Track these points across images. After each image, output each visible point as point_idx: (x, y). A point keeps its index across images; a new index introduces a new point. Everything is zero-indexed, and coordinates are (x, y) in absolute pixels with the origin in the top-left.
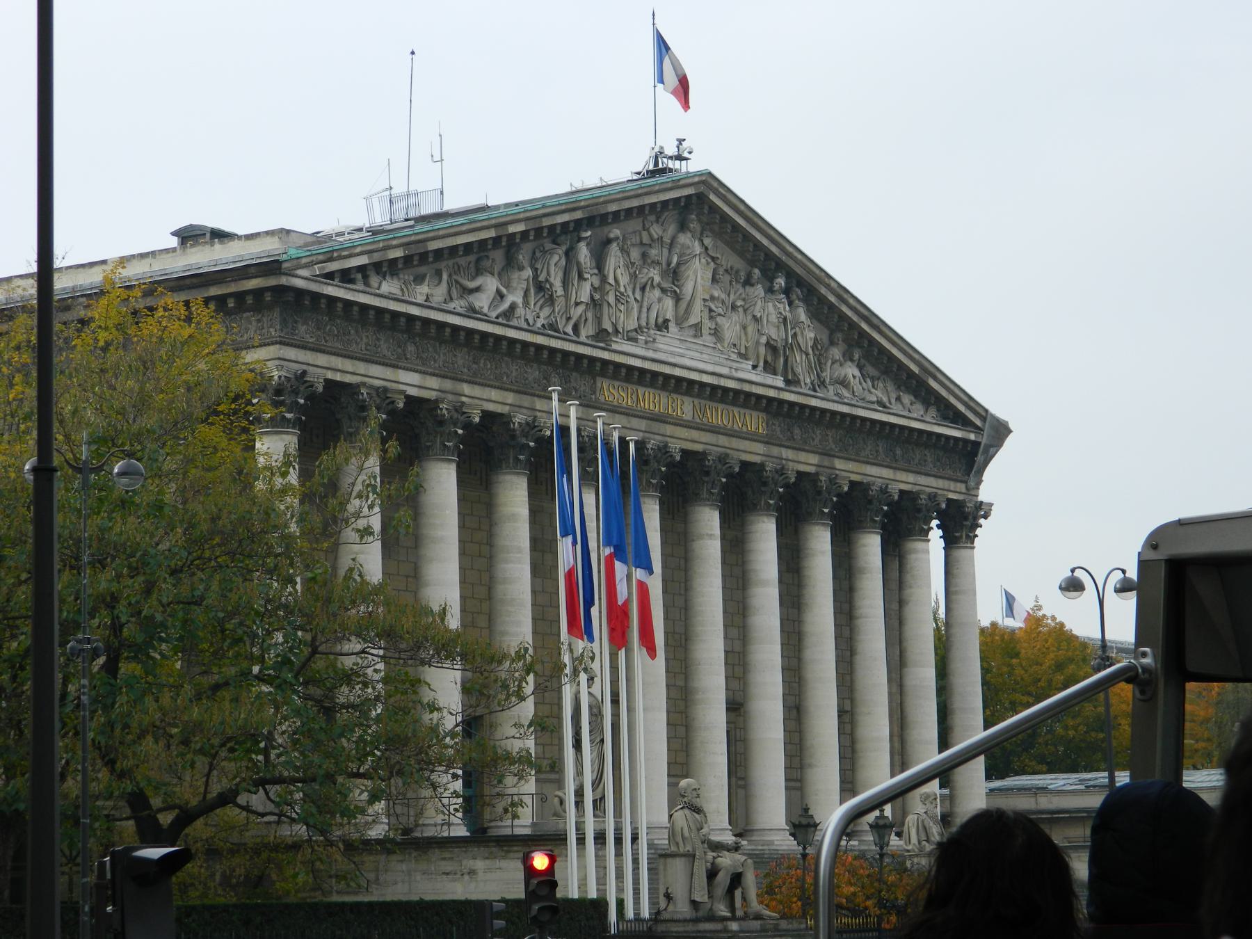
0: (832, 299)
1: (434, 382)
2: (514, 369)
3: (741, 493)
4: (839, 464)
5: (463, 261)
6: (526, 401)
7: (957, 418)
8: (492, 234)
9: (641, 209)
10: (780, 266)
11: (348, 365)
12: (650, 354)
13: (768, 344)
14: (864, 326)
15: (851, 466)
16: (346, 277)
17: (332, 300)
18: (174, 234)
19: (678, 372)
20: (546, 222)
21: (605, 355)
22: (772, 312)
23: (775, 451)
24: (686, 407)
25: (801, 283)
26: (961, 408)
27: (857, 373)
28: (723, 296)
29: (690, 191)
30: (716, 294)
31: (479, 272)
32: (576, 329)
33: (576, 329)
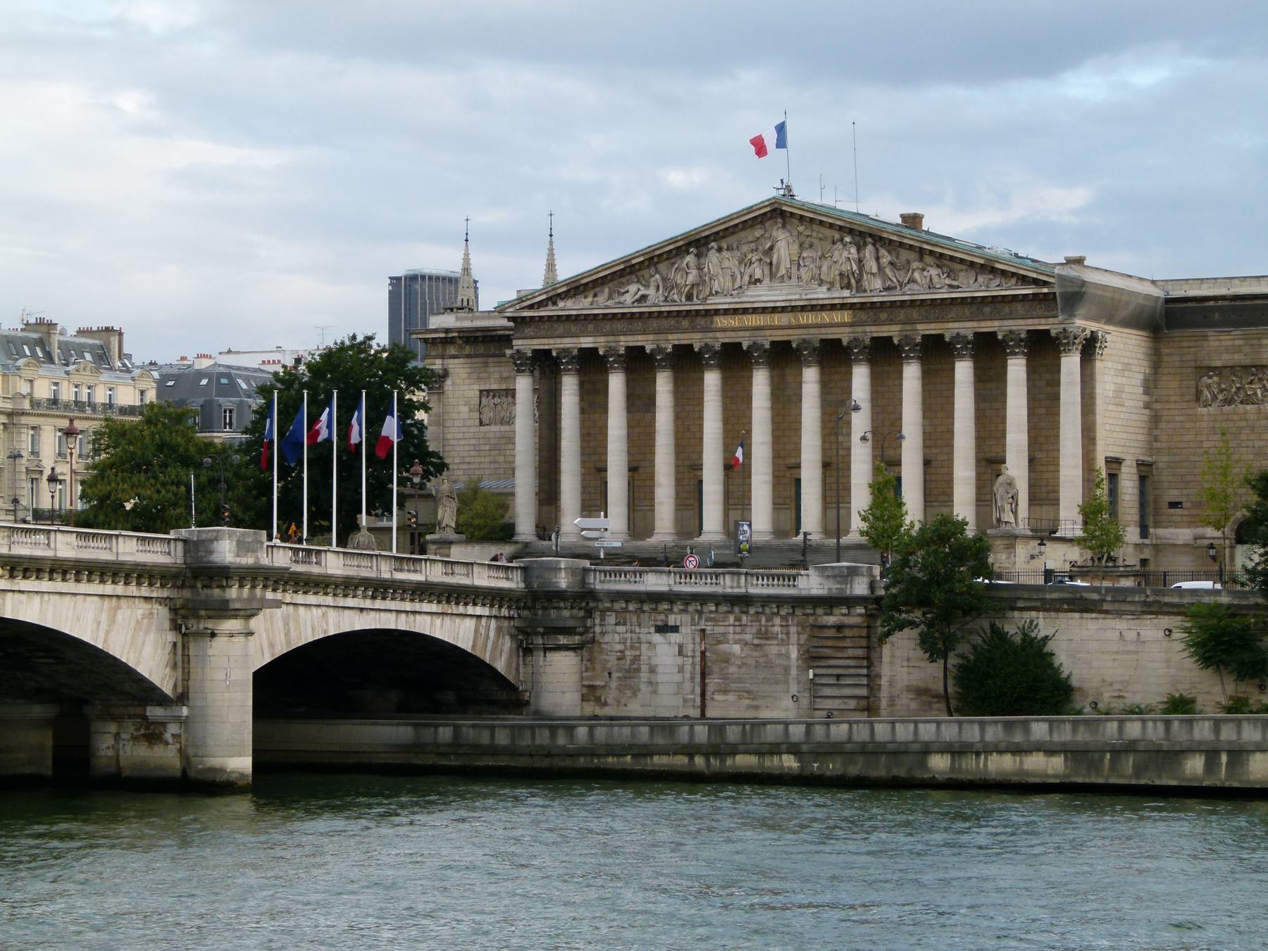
0: (895, 238)
1: (602, 339)
2: (654, 324)
3: (834, 356)
4: (919, 327)
5: (623, 280)
6: (662, 337)
7: (1036, 282)
8: (622, 266)
9: (736, 225)
10: (851, 232)
11: (551, 341)
12: (736, 300)
13: (841, 274)
14: (925, 246)
15: (932, 326)
16: (541, 304)
17: (532, 317)
18: (902, 216)
19: (756, 305)
20: (657, 253)
21: (701, 307)
22: (845, 256)
23: (860, 329)
24: (784, 319)
25: (871, 235)
26: (1035, 276)
27: (939, 271)
28: (814, 255)
29: (768, 209)
30: (805, 255)
31: (629, 283)
32: (689, 297)
33: (689, 297)
